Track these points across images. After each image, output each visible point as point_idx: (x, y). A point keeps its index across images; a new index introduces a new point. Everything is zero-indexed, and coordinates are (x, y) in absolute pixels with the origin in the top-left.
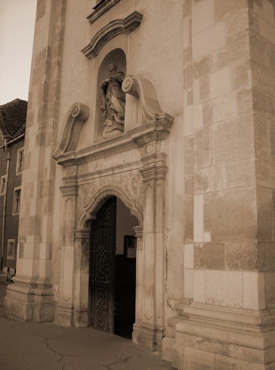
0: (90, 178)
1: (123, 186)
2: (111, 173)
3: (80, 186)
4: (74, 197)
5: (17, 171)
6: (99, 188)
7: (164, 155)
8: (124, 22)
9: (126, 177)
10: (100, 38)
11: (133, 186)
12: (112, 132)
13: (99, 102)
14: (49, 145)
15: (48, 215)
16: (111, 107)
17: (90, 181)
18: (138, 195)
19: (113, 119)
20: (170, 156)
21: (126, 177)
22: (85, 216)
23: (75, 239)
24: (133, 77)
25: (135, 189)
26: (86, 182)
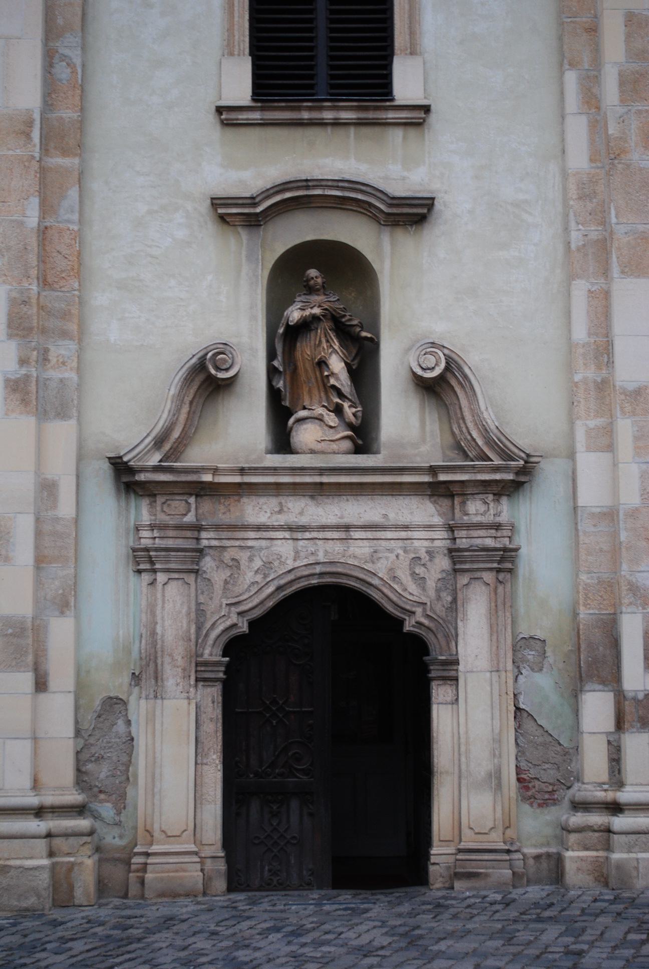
0: (252, 534)
1: (381, 568)
2: (342, 535)
3: (207, 551)
6: (290, 564)
7: (513, 527)
8: (389, 201)
9: (390, 551)
10: (288, 195)
11: (413, 574)
12: (337, 442)
13: (271, 355)
16: (332, 381)
17: (250, 543)
18: (432, 593)
19: (338, 411)
20: (522, 527)
21: (390, 551)
22: (234, 626)
24: (446, 351)
25: (420, 581)
26: (237, 543)
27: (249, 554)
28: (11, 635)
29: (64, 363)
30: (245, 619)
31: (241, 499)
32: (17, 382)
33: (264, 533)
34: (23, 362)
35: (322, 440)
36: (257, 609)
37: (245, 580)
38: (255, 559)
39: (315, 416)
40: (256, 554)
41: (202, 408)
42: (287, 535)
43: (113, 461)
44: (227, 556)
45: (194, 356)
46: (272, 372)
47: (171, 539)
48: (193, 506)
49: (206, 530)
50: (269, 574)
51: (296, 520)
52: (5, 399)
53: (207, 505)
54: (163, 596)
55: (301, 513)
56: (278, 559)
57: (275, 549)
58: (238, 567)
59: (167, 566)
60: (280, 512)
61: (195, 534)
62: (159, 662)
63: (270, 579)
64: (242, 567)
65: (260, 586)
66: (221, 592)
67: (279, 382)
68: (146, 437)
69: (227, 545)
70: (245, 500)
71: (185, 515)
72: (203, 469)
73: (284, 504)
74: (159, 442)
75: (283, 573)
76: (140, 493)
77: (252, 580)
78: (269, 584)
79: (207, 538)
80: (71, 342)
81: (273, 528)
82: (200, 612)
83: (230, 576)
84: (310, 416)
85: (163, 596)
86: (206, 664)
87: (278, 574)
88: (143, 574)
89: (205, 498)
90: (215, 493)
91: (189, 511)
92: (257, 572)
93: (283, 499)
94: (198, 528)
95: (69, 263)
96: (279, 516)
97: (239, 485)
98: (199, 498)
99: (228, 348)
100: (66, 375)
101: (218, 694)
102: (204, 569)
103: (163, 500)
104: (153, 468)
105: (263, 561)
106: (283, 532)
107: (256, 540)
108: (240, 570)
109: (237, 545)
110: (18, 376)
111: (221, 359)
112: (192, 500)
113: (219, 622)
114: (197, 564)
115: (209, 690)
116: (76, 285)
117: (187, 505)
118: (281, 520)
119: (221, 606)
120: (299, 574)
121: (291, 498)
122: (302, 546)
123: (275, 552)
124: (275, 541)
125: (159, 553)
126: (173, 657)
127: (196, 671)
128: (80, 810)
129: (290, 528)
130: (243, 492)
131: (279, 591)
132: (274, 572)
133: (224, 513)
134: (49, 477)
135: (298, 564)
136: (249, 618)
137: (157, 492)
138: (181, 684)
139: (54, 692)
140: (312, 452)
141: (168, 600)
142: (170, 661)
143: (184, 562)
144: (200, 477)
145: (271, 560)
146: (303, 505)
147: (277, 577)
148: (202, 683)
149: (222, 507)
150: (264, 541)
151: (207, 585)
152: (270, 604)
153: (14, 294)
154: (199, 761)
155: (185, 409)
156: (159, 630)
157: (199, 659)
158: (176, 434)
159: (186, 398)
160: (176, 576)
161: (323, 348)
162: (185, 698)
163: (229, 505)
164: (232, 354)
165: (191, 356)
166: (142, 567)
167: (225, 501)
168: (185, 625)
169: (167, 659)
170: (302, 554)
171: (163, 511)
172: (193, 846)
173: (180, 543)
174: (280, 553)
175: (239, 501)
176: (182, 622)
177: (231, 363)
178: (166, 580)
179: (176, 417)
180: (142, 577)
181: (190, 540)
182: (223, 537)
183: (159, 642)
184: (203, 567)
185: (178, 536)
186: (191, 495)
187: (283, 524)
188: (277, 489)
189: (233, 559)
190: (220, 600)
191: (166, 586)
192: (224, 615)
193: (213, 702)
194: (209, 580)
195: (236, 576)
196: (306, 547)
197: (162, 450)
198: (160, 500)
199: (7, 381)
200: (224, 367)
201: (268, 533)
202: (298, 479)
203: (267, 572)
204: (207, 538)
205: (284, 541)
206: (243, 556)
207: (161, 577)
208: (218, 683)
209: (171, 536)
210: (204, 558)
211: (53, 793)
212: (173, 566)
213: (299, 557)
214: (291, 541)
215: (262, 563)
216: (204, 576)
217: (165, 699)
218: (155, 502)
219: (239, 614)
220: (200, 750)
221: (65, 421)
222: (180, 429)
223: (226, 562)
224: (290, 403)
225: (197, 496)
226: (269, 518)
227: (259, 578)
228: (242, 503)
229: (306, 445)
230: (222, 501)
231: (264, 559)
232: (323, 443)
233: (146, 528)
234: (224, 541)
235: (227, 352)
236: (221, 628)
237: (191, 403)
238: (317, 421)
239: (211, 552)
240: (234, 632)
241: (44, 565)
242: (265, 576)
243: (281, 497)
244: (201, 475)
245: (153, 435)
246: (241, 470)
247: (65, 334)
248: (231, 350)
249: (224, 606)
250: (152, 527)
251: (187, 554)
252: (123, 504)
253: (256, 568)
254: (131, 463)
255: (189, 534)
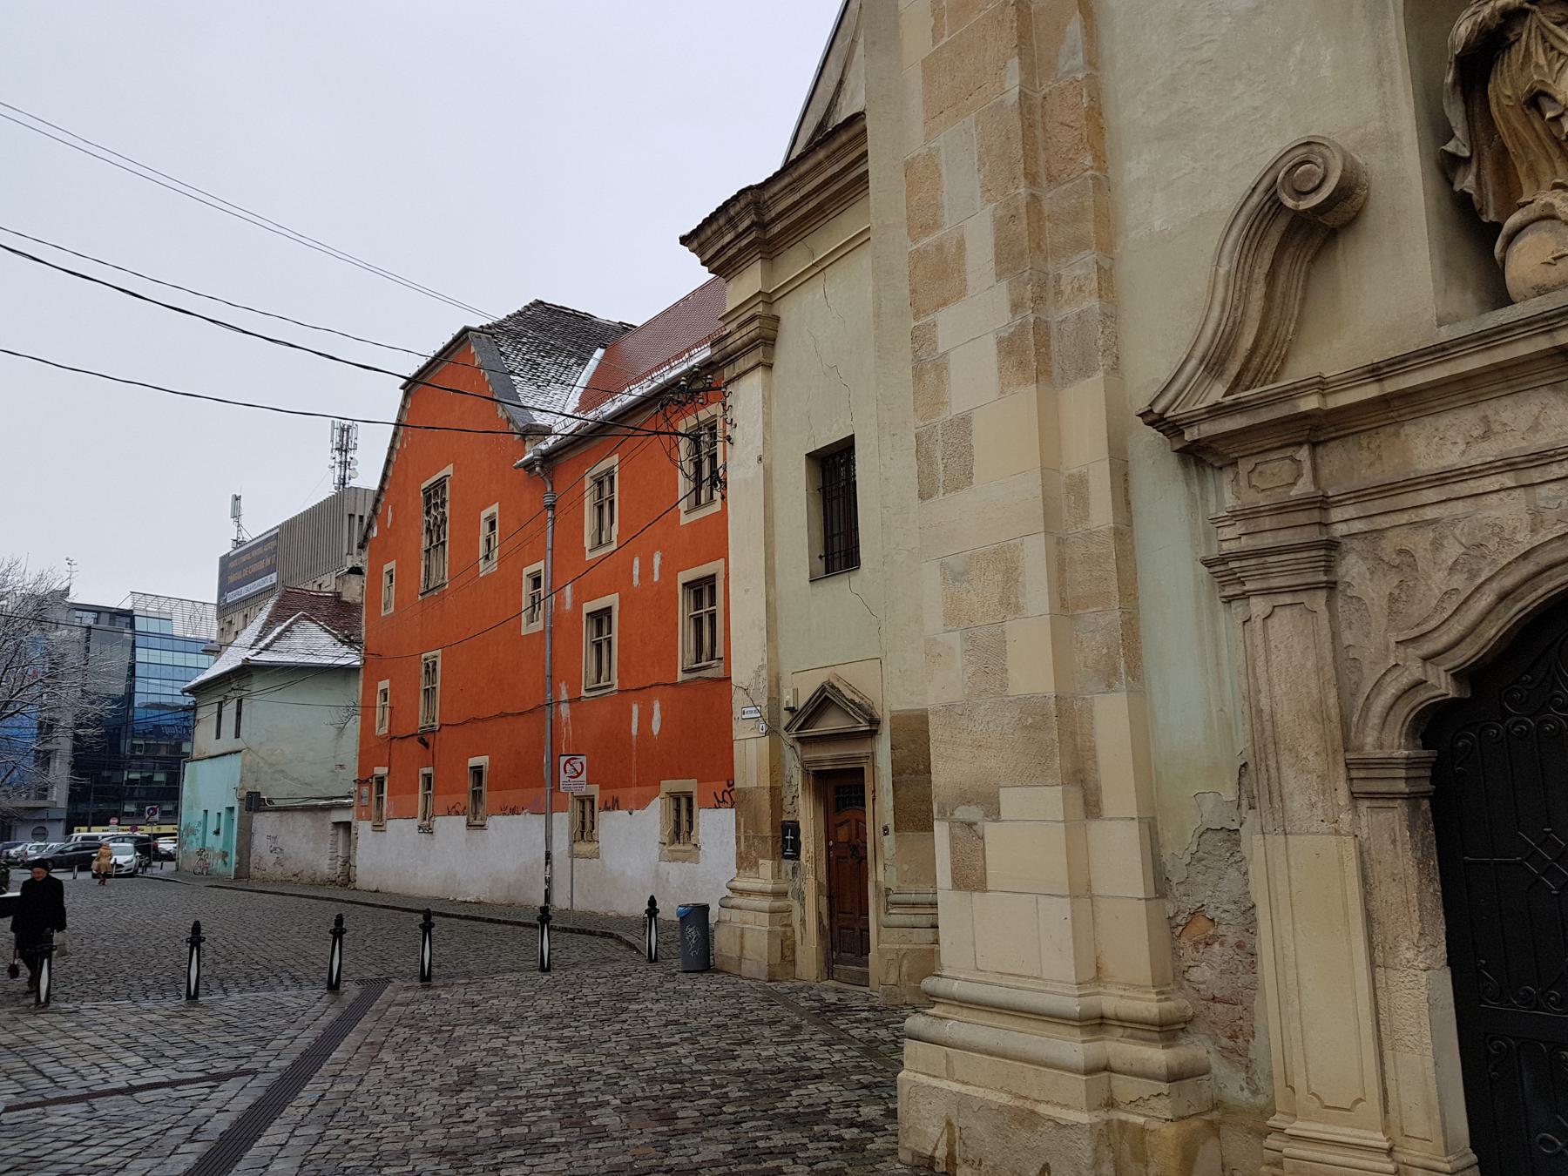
0: (1431, 495)
3: (1347, 544)
4: (1321, 597)
5: (587, 544)
6: (1525, 541)
14: (1085, 371)
15: (1130, 691)
17: (1429, 513)
22: (1419, 684)
23: (1354, 797)
27: (1431, 535)
28: (1031, 726)
29: (1080, 289)
30: (1442, 668)
31: (1402, 431)
32: (1011, 338)
33: (1457, 487)
34: (1016, 306)
35: (1555, 259)
36: (1463, 645)
37: (1430, 589)
38: (1445, 543)
39: (1537, 215)
40: (1447, 532)
41: (1307, 280)
42: (1508, 480)
43: (1150, 418)
44: (1388, 546)
45: (1254, 189)
46: (1448, 166)
47: (1269, 534)
48: (1307, 465)
49: (1339, 504)
50: (1480, 570)
51: (1524, 444)
52: (1000, 369)
53: (1335, 458)
54: (1266, 640)
55: (1535, 428)
56: (1493, 534)
57: (1486, 514)
58: (1413, 566)
59: (1265, 585)
60: (1486, 436)
61: (1315, 516)
62: (1272, 763)
63: (1483, 579)
64: (1420, 564)
65: (1462, 598)
66: (1384, 621)
67: (1465, 177)
68: (1185, 362)
69: (1384, 526)
70: (1409, 429)
71: (1294, 484)
72: (1296, 389)
73: (1492, 418)
74: (1214, 365)
75: (1510, 563)
76: (1217, 465)
77: (1445, 589)
78: (1482, 591)
79: (1344, 522)
80: (1088, 252)
81: (1470, 473)
82: (1343, 663)
83: (1397, 587)
84: (1527, 218)
85: (1266, 640)
86: (1366, 764)
87: (1500, 566)
88: (1234, 604)
89: (1331, 444)
90: (1346, 432)
91: (1300, 476)
92: (1452, 569)
93: (1487, 409)
94: (1322, 503)
95: (1076, 133)
96: (1485, 445)
97: (1385, 401)
98: (1320, 450)
99: (1315, 148)
100: (1085, 305)
101: (1401, 825)
102: (1347, 579)
103: (1251, 467)
104: (1208, 412)
105: (1462, 544)
106: (1499, 477)
107: (1442, 505)
108: (1417, 570)
109: (1404, 522)
110: (1012, 330)
111: (1303, 174)
112: (1303, 454)
113: (1388, 679)
114: (1328, 570)
115: (1383, 816)
116: (1089, 161)
117: (1294, 466)
118: (1490, 451)
119: (1387, 648)
120: (1544, 558)
121: (1507, 401)
122: (1548, 499)
123: (1485, 521)
124: (1484, 498)
125: (1245, 563)
126: (1297, 753)
127: (1350, 779)
128: (1168, 1030)
129: (1510, 465)
130: (1400, 416)
131: (1507, 602)
132: (1490, 564)
133: (1372, 464)
134: (1075, 471)
135: (1539, 539)
136: (1449, 666)
137: (1236, 455)
138: (1320, 804)
139: (1110, 819)
140: (1541, 290)
141: (1276, 646)
142: (1293, 761)
143: (1299, 572)
144: (1296, 407)
145: (1479, 540)
146: (1536, 410)
147: (1497, 573)
148: (1367, 803)
149: (1365, 454)
150: (1460, 503)
151: (1357, 610)
152: (1491, 631)
153: (1001, 212)
154: (1379, 961)
155: (1259, 291)
156: (1265, 703)
157: (1350, 756)
158: (1247, 342)
159: (1257, 271)
160: (1288, 599)
161: (1537, 65)
162: (1330, 834)
163: (1379, 446)
164: (1324, 157)
165: (1250, 191)
166: (1230, 591)
167: (1369, 443)
168: (1315, 692)
169: (1286, 758)
170: (1550, 516)
171: (1251, 486)
172: (1380, 1135)
173: (1287, 538)
174: (1497, 522)
175: (1397, 435)
176: (1307, 686)
177: (1321, 176)
178: (1269, 610)
179: (1240, 310)
180: (1233, 611)
181: (1307, 528)
182: (1374, 512)
183: (1268, 726)
184: (1343, 576)
185: (1282, 525)
186: (1300, 444)
187: (1492, 459)
188: (1467, 388)
189: (1400, 552)
190: (1384, 637)
191: (1269, 621)
192: (1397, 665)
193: (1394, 842)
194: (1360, 599)
195: (1411, 584)
196: (1555, 498)
197: (1225, 377)
198: (1245, 466)
199: (1000, 342)
200: (1311, 186)
201: (1464, 485)
202: (1500, 356)
203: (1475, 567)
204: (1344, 522)
205: (1502, 493)
206: (1420, 542)
207: (1258, 606)
208: (1399, 801)
209: (1267, 528)
210: (1344, 558)
211: (1122, 993)
212: (1276, 582)
213: (1542, 522)
214: (1519, 491)
215: (1463, 550)
216: (1349, 592)
217: (1290, 833)
218: (1238, 473)
219: (1425, 659)
220: (1377, 939)
221: (1089, 377)
222: (1254, 332)
223: (1386, 559)
224: (1497, 214)
225: (1314, 446)
226: (1463, 453)
227: (1458, 581)
228: (1403, 438)
229: (1524, 281)
230: (1364, 443)
231: (1464, 541)
232: (1560, 264)
233: (1227, 523)
234: (1378, 519)
235: (1312, 157)
236: (1391, 691)
237: (1271, 276)
238: (1544, 223)
239: (1357, 544)
240: (1422, 696)
241: (1080, 612)
242: (1473, 575)
243: (1484, 406)
244: (1294, 402)
245: (1198, 354)
246: (1373, 370)
247: (1079, 244)
248: (1322, 148)
249: (1393, 646)
250: (1235, 516)
251: (1299, 555)
252: (1196, 489)
253: (1450, 563)
254: (1170, 413)
255: (1302, 518)
